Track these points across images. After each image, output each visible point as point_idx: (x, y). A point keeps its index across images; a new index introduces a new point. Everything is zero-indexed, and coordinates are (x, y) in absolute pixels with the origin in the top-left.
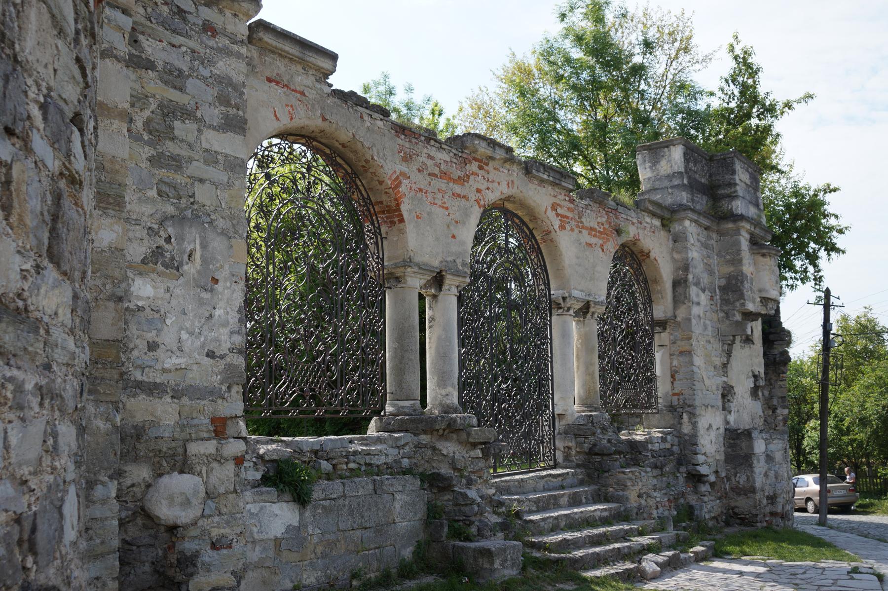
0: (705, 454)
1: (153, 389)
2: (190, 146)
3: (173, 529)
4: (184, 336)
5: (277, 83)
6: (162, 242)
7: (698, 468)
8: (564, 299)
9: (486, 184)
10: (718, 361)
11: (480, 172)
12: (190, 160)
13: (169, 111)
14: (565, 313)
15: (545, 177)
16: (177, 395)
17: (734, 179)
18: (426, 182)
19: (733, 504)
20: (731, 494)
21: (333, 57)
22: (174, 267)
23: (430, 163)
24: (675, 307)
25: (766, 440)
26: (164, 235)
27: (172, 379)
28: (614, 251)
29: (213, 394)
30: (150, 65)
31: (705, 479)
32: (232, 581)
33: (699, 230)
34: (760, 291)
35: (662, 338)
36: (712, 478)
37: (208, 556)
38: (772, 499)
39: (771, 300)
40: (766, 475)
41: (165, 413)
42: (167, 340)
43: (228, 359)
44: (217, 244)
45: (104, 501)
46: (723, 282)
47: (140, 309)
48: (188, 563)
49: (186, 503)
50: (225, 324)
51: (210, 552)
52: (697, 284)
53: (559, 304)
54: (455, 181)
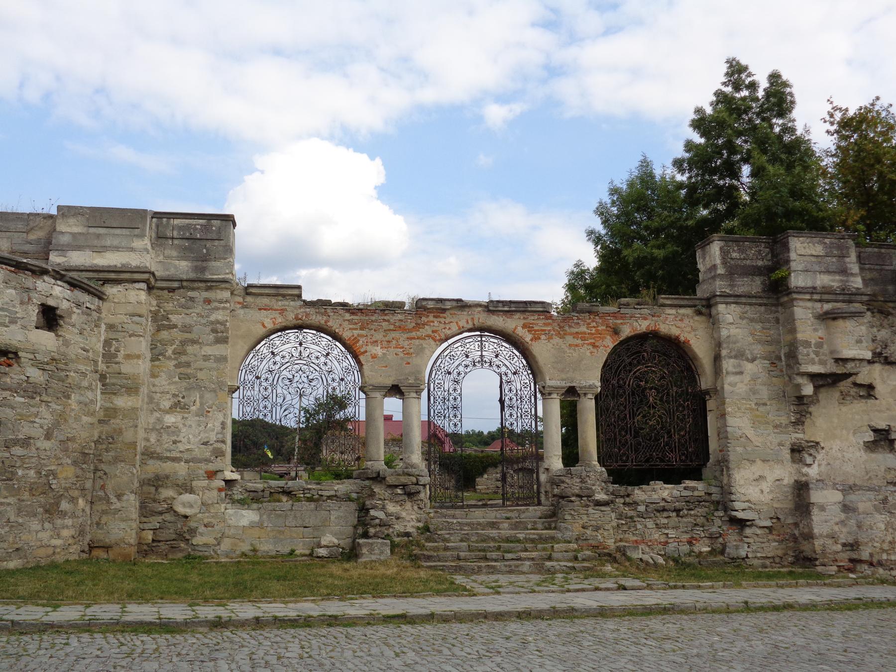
0: (748, 501)
1: (174, 460)
2: (195, 355)
3: (186, 517)
4: (191, 436)
5: (265, 309)
6: (180, 399)
7: (734, 513)
9: (442, 326)
10: (784, 420)
11: (435, 319)
12: (196, 361)
15: (506, 309)
16: (187, 462)
17: (789, 257)
18: (381, 336)
19: (802, 548)
20: (800, 539)
21: (299, 287)
23: (384, 324)
24: (716, 379)
25: (842, 491)
26: (181, 395)
27: (186, 456)
28: (612, 346)
29: (207, 461)
30: (175, 326)
31: (748, 523)
32: (215, 542)
33: (748, 308)
34: (832, 352)
35: (711, 404)
36: (768, 523)
37: (202, 529)
38: (853, 546)
39: (853, 360)
40: (842, 523)
41: (181, 469)
42: (183, 440)
43: (215, 445)
44: (208, 396)
45: (128, 500)
46: (787, 349)
47: (169, 427)
48: (193, 531)
49: (191, 506)
50: (213, 430)
51: (203, 528)
52: (740, 355)
54: (410, 331)
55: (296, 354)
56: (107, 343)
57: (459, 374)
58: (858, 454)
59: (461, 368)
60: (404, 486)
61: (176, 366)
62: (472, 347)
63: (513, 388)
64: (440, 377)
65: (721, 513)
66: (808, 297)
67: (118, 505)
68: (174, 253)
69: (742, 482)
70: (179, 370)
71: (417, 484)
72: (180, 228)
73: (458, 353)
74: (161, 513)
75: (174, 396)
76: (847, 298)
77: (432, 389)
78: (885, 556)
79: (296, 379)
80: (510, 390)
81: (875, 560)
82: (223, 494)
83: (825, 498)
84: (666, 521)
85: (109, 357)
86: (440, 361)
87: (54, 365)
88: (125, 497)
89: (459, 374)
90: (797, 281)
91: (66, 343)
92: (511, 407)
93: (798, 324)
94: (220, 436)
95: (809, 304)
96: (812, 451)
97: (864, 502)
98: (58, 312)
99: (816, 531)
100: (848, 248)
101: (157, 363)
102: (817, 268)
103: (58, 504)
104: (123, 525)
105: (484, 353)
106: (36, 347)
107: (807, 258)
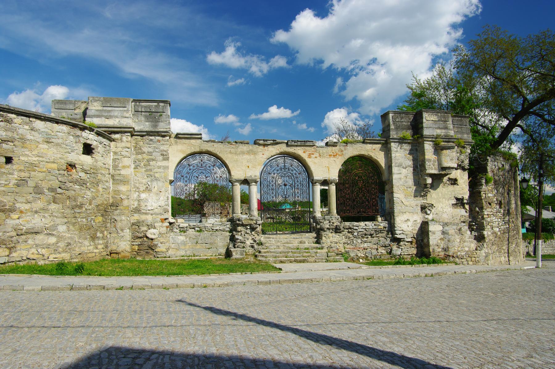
1: (146, 214)
3: (152, 239)
7: (396, 236)
13: (148, 161)
21: (201, 134)
22: (150, 190)
27: (151, 212)
30: (144, 153)
35: (387, 187)
36: (410, 240)
37: (160, 245)
38: (445, 250)
41: (149, 219)
46: (420, 163)
52: (400, 166)
55: (200, 165)
56: (114, 160)
57: (274, 174)
58: (449, 209)
59: (275, 171)
60: (250, 225)
61: (146, 171)
65: (391, 236)
66: (430, 139)
67: (122, 234)
68: (143, 119)
69: (400, 222)
70: (146, 173)
72: (145, 107)
74: (141, 238)
75: (145, 184)
76: (447, 140)
78: (459, 253)
79: (200, 177)
80: (298, 181)
81: (455, 255)
82: (169, 229)
83: (435, 229)
84: (366, 239)
85: (115, 167)
87: (92, 172)
88: (125, 231)
90: (426, 132)
91: (96, 161)
93: (425, 151)
94: (166, 203)
95: (431, 143)
96: (430, 208)
97: (451, 230)
98: (92, 146)
99: (431, 243)
100: (448, 118)
101: (137, 170)
102: (435, 126)
103: (96, 234)
104: (125, 243)
106: (83, 163)
107: (430, 122)
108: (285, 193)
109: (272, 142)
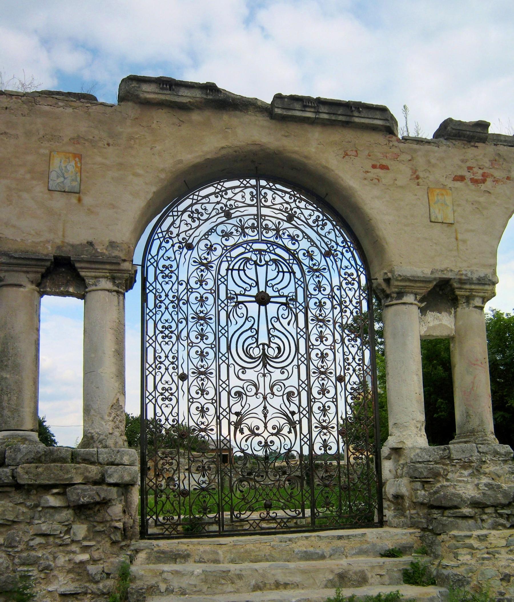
8: (388, 281)
14: (394, 302)
53: (383, 291)
57: (210, 249)
59: (214, 238)
62: (238, 197)
63: (324, 282)
64: (170, 254)
71: (101, 481)
73: (210, 207)
77: (151, 278)
80: (319, 287)
86: (169, 220)
89: (210, 249)
92: (321, 320)
105: (264, 211)
108: (263, 338)
109: (198, 94)
